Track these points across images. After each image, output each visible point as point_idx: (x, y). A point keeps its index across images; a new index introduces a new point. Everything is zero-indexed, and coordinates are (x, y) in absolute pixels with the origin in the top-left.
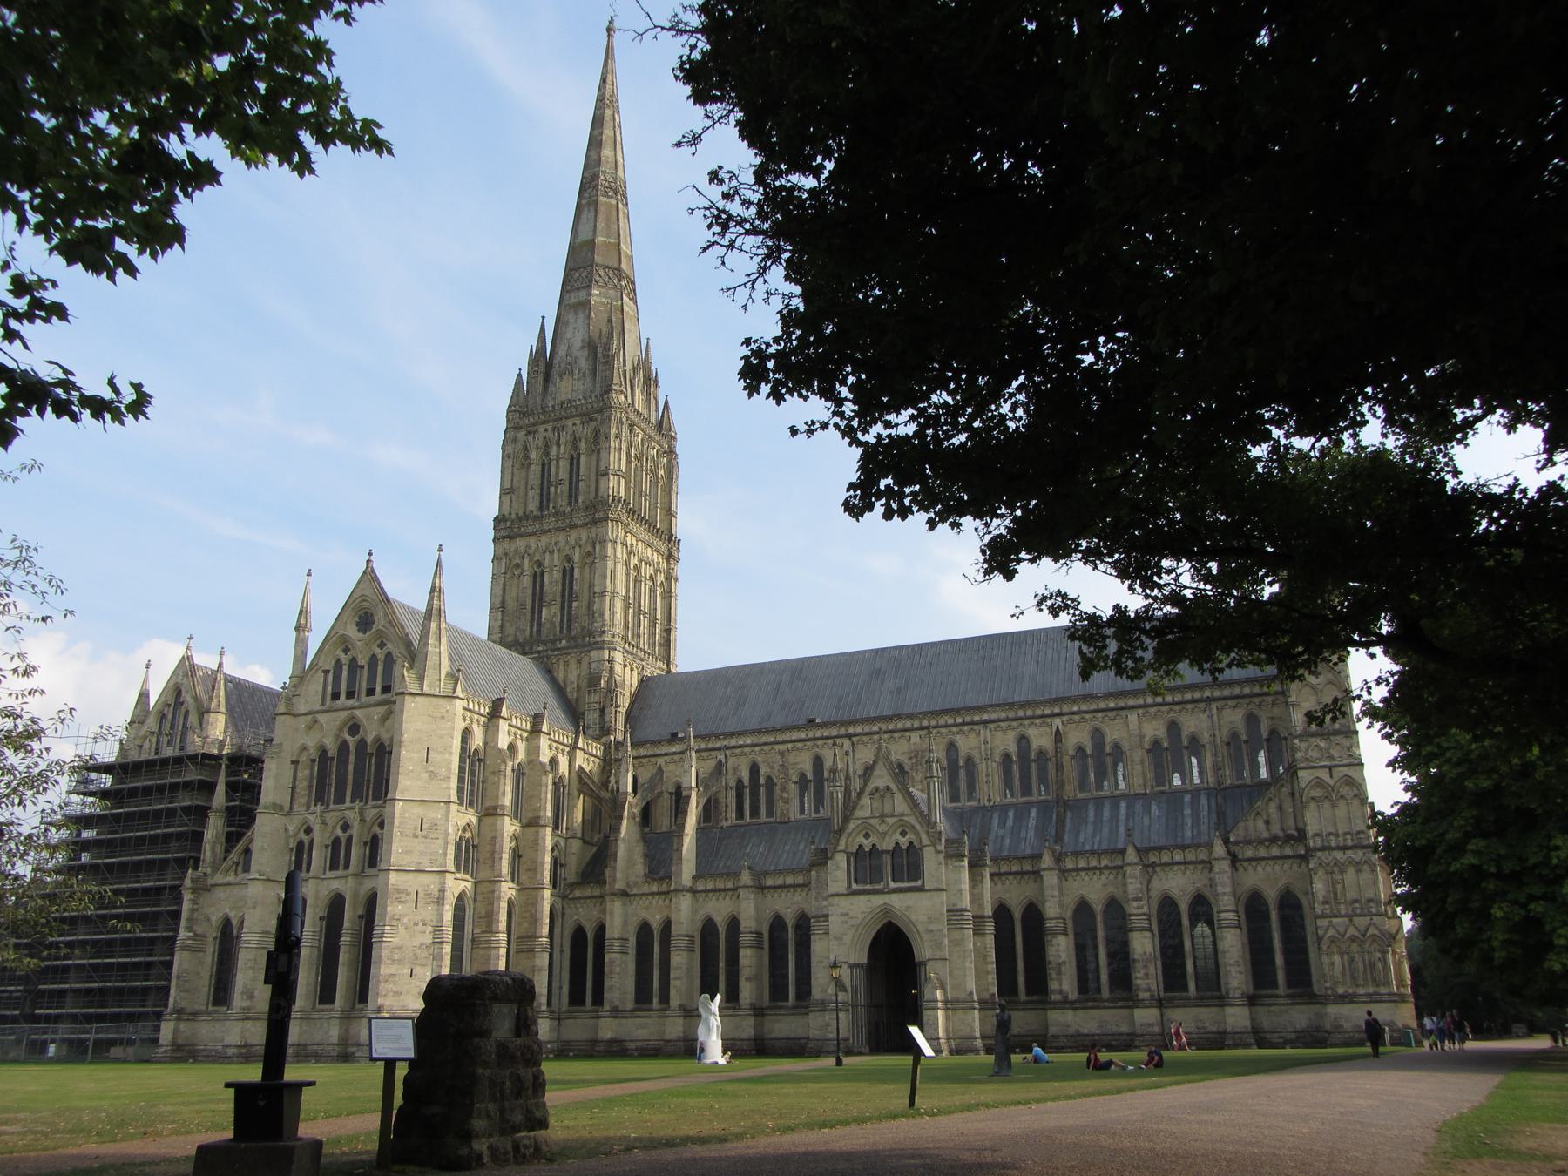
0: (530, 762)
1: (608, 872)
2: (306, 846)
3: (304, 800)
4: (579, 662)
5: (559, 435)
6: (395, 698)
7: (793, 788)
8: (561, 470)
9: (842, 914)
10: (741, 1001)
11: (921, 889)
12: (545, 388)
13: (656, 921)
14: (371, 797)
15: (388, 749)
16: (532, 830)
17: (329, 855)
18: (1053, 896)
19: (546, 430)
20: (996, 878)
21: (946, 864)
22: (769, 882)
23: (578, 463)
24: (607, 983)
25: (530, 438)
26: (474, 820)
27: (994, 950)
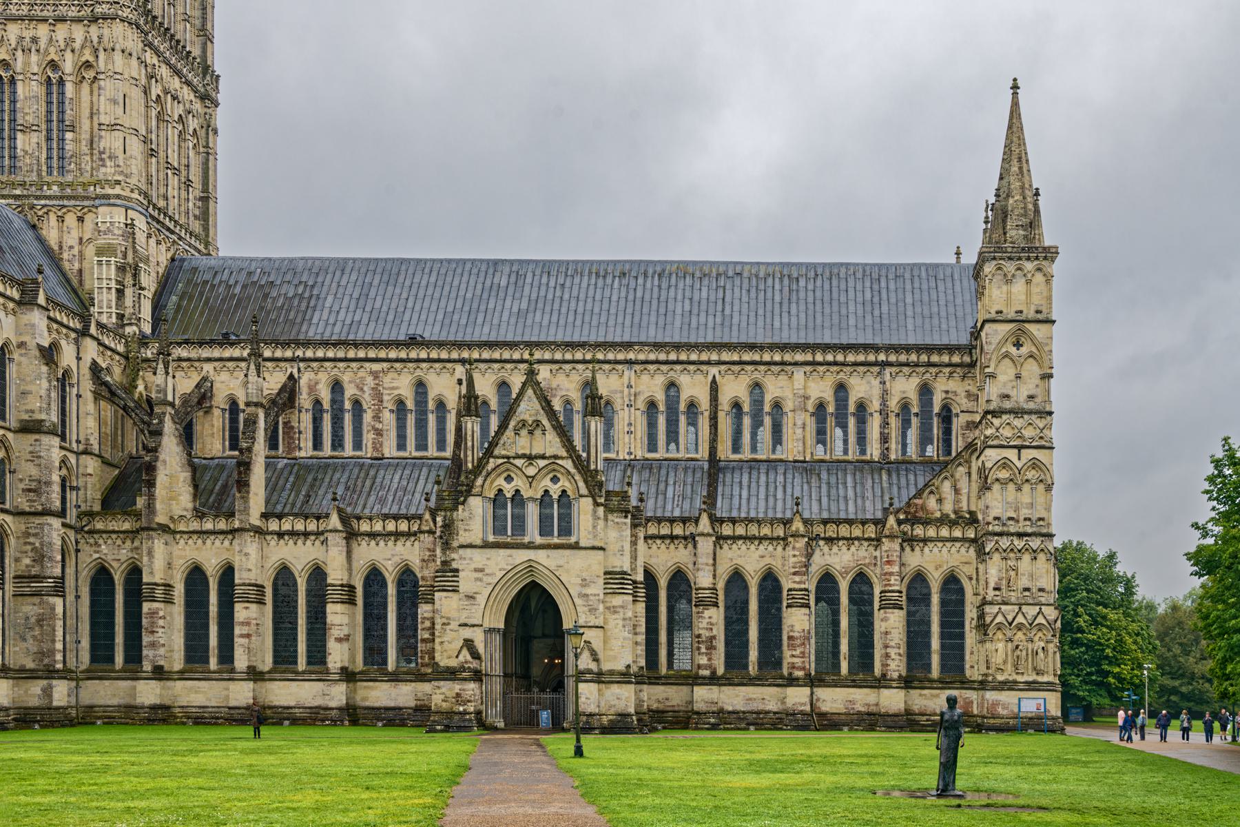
1: (141, 502)
4: (81, 219)
7: (389, 418)
9: (476, 570)
10: (330, 665)
11: (576, 546)
13: (212, 567)
18: (707, 564)
20: (650, 542)
21: (606, 519)
22: (365, 527)
24: (146, 639)
27: (644, 620)
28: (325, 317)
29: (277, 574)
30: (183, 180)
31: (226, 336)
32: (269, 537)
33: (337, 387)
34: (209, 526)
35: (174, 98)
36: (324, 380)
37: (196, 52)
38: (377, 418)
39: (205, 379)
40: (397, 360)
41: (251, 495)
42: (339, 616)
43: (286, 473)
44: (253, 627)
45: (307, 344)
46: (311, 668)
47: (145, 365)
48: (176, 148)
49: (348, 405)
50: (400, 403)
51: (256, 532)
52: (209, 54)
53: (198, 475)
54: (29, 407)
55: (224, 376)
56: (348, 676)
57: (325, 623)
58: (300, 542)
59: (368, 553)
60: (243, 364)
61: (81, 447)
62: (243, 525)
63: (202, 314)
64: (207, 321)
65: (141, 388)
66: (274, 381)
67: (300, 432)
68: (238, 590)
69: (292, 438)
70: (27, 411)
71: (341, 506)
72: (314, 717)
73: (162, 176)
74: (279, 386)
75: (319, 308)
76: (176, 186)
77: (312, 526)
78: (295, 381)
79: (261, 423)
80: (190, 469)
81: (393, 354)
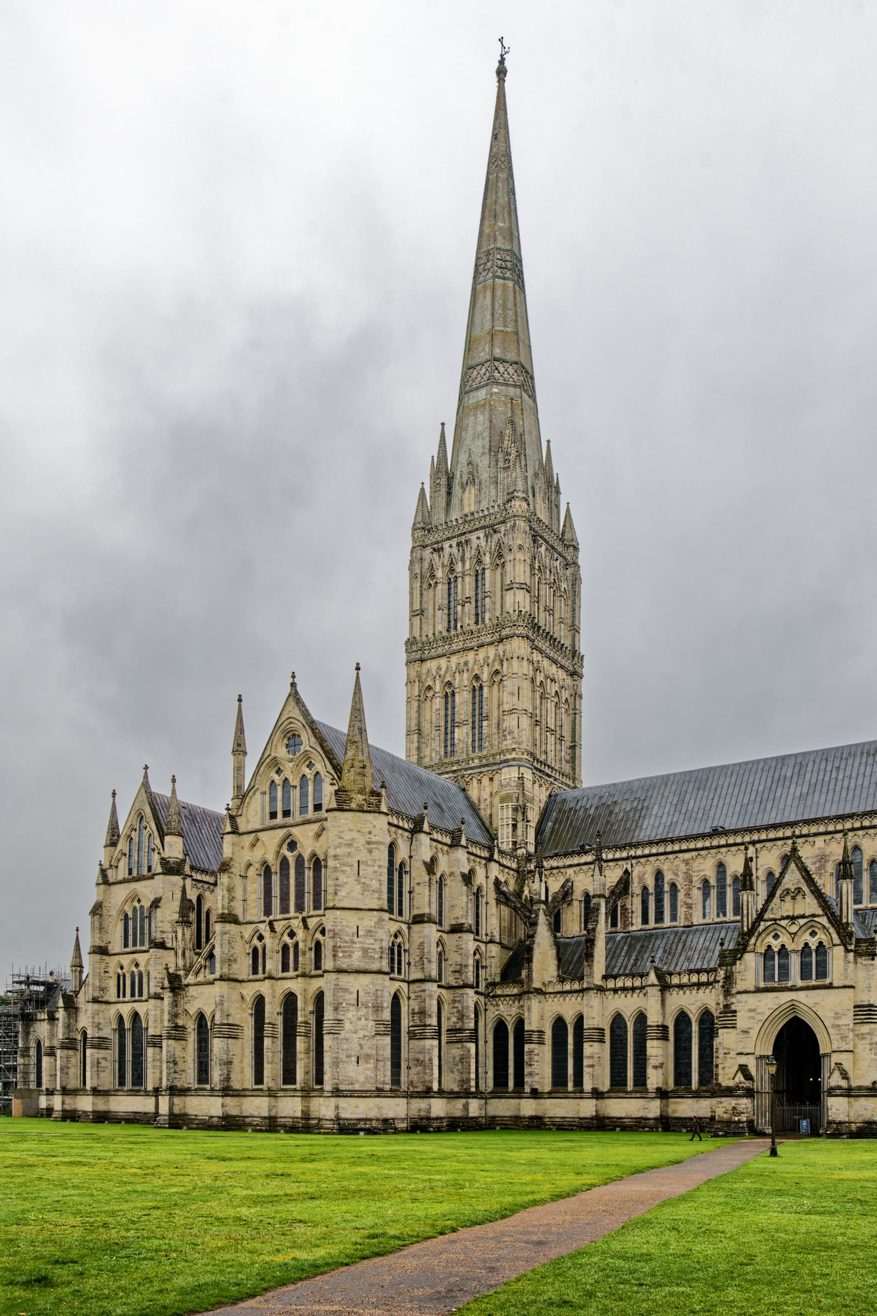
0: (452, 874)
2: (260, 952)
3: (254, 911)
5: (463, 550)
6: (326, 815)
7: (697, 894)
8: (467, 586)
12: (448, 503)
14: (312, 908)
15: (323, 863)
16: (457, 935)
17: (280, 959)
19: (451, 546)
23: (483, 579)
25: (435, 555)
26: (404, 927)
28: (652, 823)
29: (614, 1019)
30: (558, 736)
31: (582, 847)
32: (607, 993)
33: (659, 876)
34: (567, 987)
35: (552, 680)
36: (649, 871)
37: (567, 642)
38: (688, 895)
39: (567, 881)
40: (703, 849)
41: (595, 963)
42: (655, 1049)
43: (622, 943)
44: (596, 1060)
45: (637, 845)
46: (637, 1088)
47: (530, 876)
48: (553, 715)
49: (667, 888)
50: (706, 882)
51: (598, 990)
52: (577, 642)
53: (562, 951)
54: (455, 916)
55: (581, 876)
56: (662, 1094)
57: (645, 1055)
58: (629, 995)
59: (678, 1000)
60: (592, 866)
61: (489, 938)
62: (589, 986)
63: (568, 832)
64: (570, 838)
65: (526, 892)
66: (613, 875)
67: (632, 912)
68: (586, 1033)
69: (627, 917)
70: (454, 918)
71: (660, 966)
72: (637, 1126)
73: (543, 737)
74: (618, 879)
75: (647, 816)
76: (553, 743)
77: (637, 983)
78: (629, 874)
79: (603, 910)
80: (555, 947)
81: (700, 844)
